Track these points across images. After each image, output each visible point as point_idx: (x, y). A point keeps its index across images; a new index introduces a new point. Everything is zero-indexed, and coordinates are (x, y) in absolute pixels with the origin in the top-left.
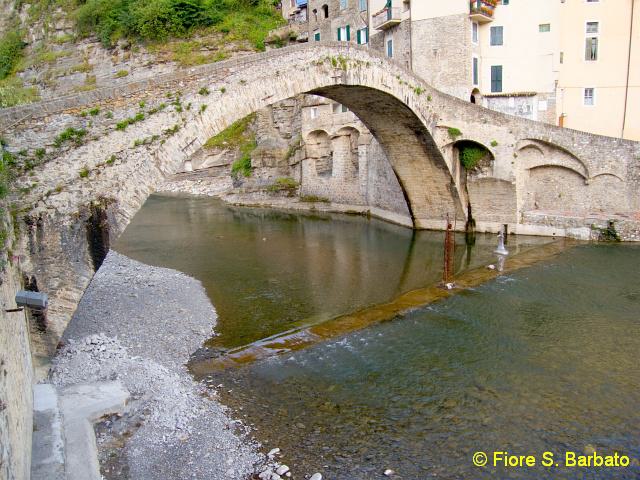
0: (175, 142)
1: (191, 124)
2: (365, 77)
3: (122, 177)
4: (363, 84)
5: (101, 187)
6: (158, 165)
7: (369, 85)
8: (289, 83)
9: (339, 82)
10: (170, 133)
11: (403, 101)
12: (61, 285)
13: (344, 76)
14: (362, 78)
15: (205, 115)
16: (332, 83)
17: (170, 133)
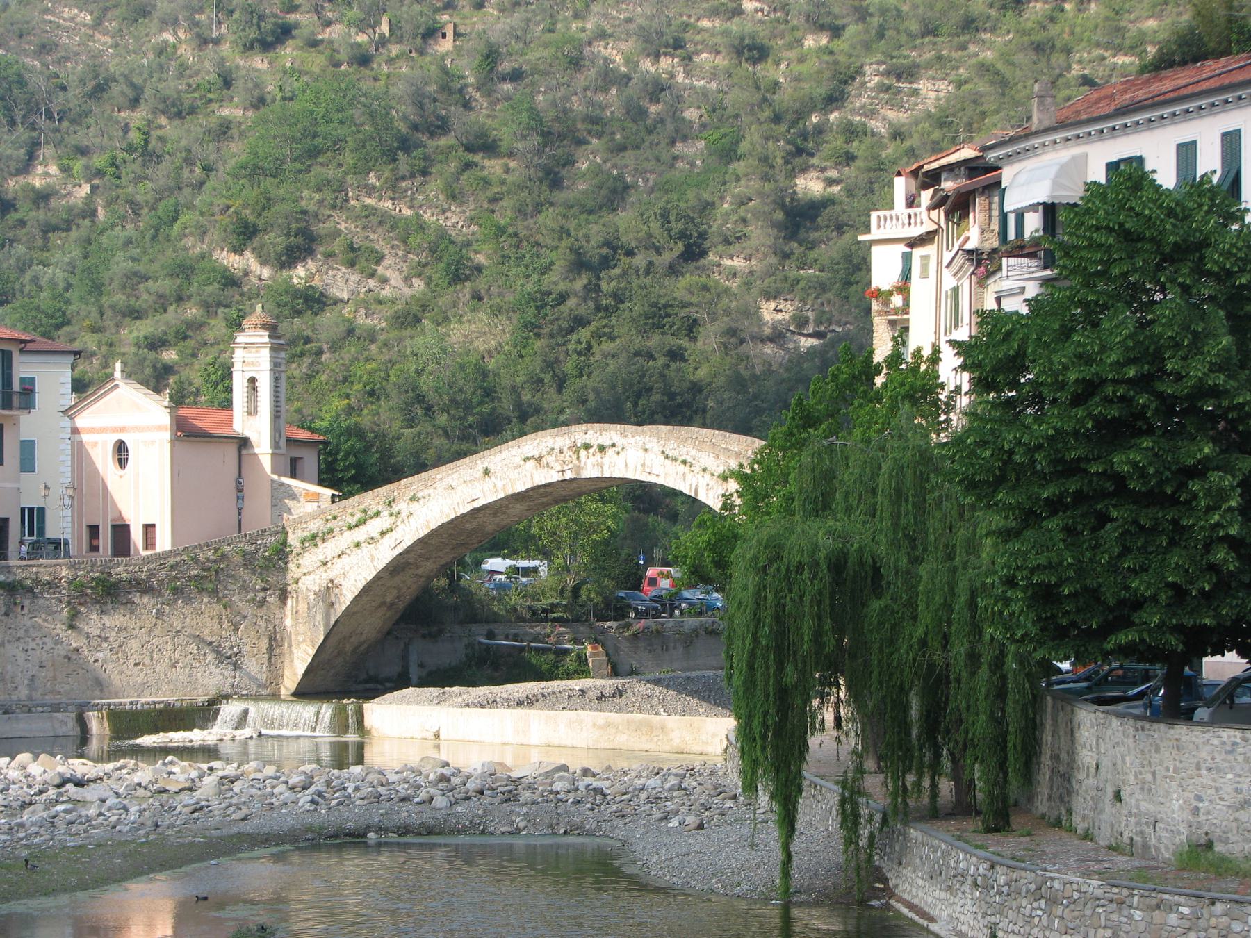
0: (389, 540)
1: (401, 527)
2: (612, 465)
3: (347, 568)
4: (607, 475)
5: (334, 571)
6: (372, 559)
7: (617, 475)
8: (500, 484)
9: (569, 475)
10: (383, 533)
11: (686, 491)
12: (304, 641)
13: (578, 469)
14: (605, 468)
15: (412, 520)
16: (555, 477)
17: (383, 533)
